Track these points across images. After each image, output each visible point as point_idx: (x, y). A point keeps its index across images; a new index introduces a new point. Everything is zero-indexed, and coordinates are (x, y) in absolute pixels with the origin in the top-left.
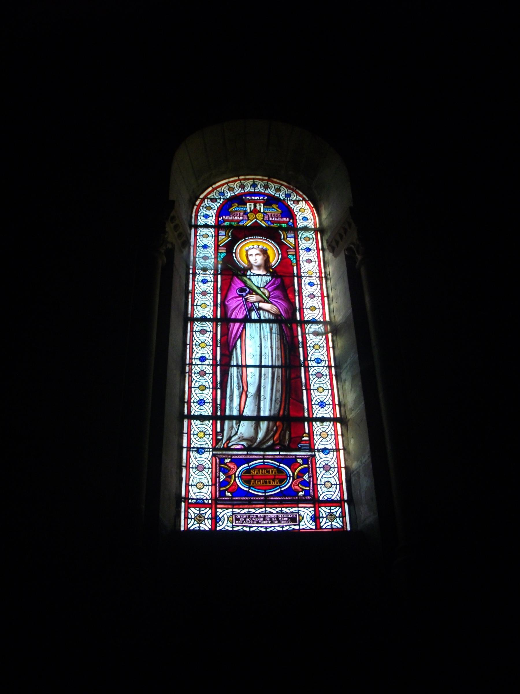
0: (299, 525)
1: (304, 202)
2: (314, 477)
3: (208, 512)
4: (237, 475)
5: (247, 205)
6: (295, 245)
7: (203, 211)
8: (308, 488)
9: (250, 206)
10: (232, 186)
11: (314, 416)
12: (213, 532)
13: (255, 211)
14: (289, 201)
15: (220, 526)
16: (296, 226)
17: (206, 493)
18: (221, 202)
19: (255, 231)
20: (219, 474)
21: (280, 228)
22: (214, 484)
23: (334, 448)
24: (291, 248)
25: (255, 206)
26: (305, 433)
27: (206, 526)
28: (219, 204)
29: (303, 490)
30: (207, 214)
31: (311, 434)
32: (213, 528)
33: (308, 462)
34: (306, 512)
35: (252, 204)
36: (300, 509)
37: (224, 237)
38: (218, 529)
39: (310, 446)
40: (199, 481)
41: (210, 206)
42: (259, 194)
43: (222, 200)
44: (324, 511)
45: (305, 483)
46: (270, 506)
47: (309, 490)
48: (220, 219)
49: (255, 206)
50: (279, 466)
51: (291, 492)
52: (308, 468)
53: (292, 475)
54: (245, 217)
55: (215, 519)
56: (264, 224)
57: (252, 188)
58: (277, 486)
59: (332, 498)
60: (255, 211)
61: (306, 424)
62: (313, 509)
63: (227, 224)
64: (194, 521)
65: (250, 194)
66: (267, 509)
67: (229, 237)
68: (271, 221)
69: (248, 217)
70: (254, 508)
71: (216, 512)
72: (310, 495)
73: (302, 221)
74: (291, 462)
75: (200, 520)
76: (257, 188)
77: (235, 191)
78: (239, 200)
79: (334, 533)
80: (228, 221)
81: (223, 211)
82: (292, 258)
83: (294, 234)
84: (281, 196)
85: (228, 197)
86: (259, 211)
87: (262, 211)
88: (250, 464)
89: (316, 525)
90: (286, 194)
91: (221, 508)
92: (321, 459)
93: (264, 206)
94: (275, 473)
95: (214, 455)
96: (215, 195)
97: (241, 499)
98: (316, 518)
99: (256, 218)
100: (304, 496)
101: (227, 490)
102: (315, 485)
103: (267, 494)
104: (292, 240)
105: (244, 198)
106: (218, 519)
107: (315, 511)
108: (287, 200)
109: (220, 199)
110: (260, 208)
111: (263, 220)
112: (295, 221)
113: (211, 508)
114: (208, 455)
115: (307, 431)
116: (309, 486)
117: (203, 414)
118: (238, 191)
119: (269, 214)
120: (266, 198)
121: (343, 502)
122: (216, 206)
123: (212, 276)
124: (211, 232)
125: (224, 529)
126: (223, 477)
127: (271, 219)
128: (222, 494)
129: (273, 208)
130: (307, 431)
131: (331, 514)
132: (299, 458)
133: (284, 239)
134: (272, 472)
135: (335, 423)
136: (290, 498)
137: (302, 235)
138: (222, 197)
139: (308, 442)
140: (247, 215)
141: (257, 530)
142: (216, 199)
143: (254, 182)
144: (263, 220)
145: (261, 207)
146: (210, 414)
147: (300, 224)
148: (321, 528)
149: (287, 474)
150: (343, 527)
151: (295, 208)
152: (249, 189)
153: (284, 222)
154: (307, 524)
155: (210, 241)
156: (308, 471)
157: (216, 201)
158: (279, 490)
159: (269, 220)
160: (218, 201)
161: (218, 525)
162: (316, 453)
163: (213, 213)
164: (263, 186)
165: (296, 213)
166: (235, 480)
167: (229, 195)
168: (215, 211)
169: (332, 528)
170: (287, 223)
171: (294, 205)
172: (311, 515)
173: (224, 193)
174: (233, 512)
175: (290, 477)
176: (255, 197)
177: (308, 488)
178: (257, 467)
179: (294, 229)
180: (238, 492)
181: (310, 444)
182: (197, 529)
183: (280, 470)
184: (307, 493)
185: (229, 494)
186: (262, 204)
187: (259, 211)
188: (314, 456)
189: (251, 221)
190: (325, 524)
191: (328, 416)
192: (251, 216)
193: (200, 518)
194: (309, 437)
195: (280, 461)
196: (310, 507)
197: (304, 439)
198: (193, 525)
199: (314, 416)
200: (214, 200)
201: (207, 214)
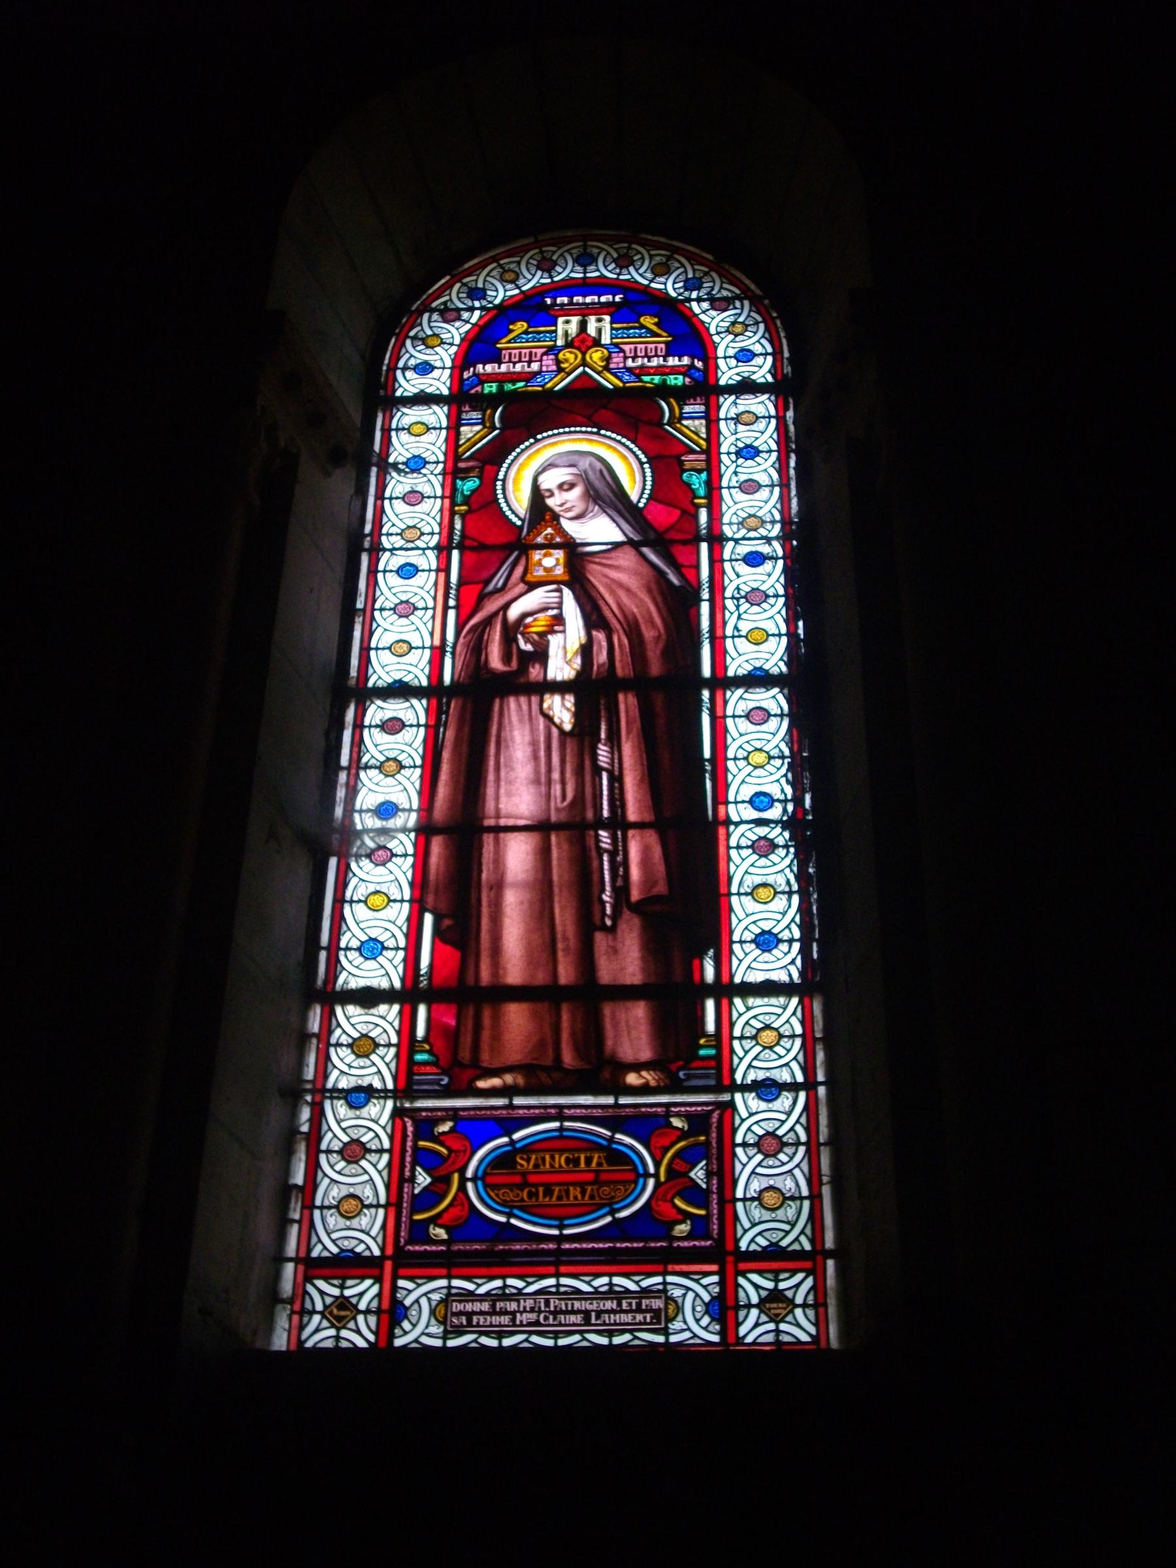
0: (666, 1332)
1: (746, 303)
2: (724, 1175)
3: (365, 1292)
4: (469, 1173)
5: (555, 325)
6: (707, 440)
7: (415, 354)
8: (703, 1212)
9: (568, 326)
10: (512, 266)
11: (737, 980)
12: (382, 1352)
13: (583, 342)
14: (694, 305)
15: (406, 1333)
16: (712, 381)
17: (367, 1234)
18: (474, 320)
19: (583, 405)
20: (413, 1171)
21: (664, 391)
22: (393, 1204)
23: (800, 1078)
24: (693, 452)
25: (583, 326)
26: (704, 1034)
27: (360, 1335)
28: (468, 326)
29: (687, 1216)
30: (429, 362)
31: (722, 1039)
32: (382, 1344)
33: (709, 1126)
34: (693, 1292)
35: (575, 320)
36: (670, 1279)
37: (478, 428)
38: (398, 1342)
39: (719, 1076)
40: (351, 1194)
41: (437, 336)
42: (601, 286)
43: (477, 314)
44: (753, 1286)
45: (695, 1195)
46: (572, 1269)
47: (708, 1216)
48: (466, 375)
49: (583, 326)
50: (611, 1140)
51: (650, 1223)
52: (708, 1143)
53: (652, 1170)
54: (549, 361)
55: (392, 1313)
56: (608, 382)
57: (578, 268)
58: (601, 1206)
59: (784, 1243)
60: (583, 342)
61: (710, 1005)
62: (715, 1278)
63: (491, 388)
64: (329, 1324)
65: (570, 287)
66: (564, 1281)
67: (494, 428)
68: (630, 370)
69: (558, 362)
70: (520, 1277)
71: (395, 1288)
72: (707, 1236)
73: (733, 362)
74: (647, 1126)
75: (339, 1319)
76: (593, 267)
77: (521, 281)
78: (535, 309)
79: (782, 1354)
80: (491, 378)
81: (480, 346)
82: (697, 482)
83: (707, 405)
84: (671, 286)
85: (497, 302)
86: (597, 342)
87: (606, 339)
88: (516, 1136)
89: (722, 1333)
90: (686, 281)
91: (411, 1278)
92: (753, 1115)
93: (612, 322)
94: (599, 1164)
95: (397, 1113)
96: (456, 297)
97: (480, 1247)
98: (724, 1308)
99: (584, 363)
100: (690, 1236)
101: (434, 1220)
102: (727, 1200)
103: (566, 1232)
104: (700, 425)
105: (549, 301)
106: (401, 1311)
107: (721, 1283)
108: (689, 300)
109: (472, 309)
110: (599, 331)
111: (606, 368)
112: (711, 362)
113: (378, 1279)
114: (380, 1111)
115: (711, 1027)
116: (705, 1205)
117: (374, 983)
118: (532, 280)
119: (626, 348)
120: (618, 298)
121: (819, 1258)
122: (455, 332)
123: (432, 555)
124: (438, 415)
125: (414, 1345)
126: (423, 1179)
127: (630, 363)
128: (419, 1232)
129: (642, 327)
130: (711, 1027)
131: (775, 1296)
132: (678, 1115)
133: (669, 424)
134: (588, 1161)
135: (806, 1000)
136: (645, 1244)
137: (728, 406)
138: (477, 304)
139: (713, 1063)
140: (556, 355)
141: (526, 1345)
142: (458, 310)
143: (585, 247)
144: (606, 368)
145: (602, 327)
146: (397, 984)
147: (728, 374)
148: (739, 1340)
149: (635, 1169)
150: (815, 1339)
151: (714, 321)
152: (568, 271)
153: (674, 370)
154: (694, 1327)
155: (433, 446)
156: (707, 1156)
157: (459, 318)
158: (609, 1219)
159: (625, 367)
160: (465, 315)
161: (397, 1331)
162: (738, 1097)
163: (444, 357)
164: (615, 261)
165: (716, 339)
166: (462, 1188)
167: (500, 294)
168: (454, 349)
169: (778, 1343)
170: (686, 371)
171: (714, 313)
172: (707, 1298)
173: (484, 290)
174: (449, 1287)
175: (647, 1175)
176: (585, 296)
177: (703, 1212)
178: (538, 1146)
179: (706, 389)
180: (469, 1224)
181: (719, 1068)
182: (329, 1344)
183: (618, 1157)
184: (700, 1227)
185: (441, 1233)
186: (607, 318)
187: (597, 342)
188: (732, 1105)
189: (569, 374)
190: (753, 1328)
191: (784, 978)
192: (569, 356)
193: (342, 1312)
194: (718, 1046)
195: (616, 1121)
196: (706, 1274)
197: (702, 1052)
198: (319, 1334)
199: (737, 980)
200: (450, 314)
201: (426, 363)
